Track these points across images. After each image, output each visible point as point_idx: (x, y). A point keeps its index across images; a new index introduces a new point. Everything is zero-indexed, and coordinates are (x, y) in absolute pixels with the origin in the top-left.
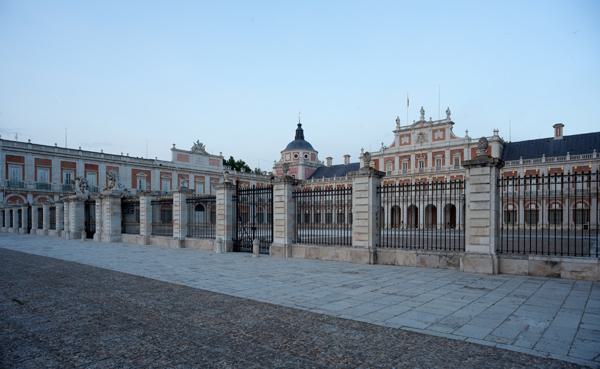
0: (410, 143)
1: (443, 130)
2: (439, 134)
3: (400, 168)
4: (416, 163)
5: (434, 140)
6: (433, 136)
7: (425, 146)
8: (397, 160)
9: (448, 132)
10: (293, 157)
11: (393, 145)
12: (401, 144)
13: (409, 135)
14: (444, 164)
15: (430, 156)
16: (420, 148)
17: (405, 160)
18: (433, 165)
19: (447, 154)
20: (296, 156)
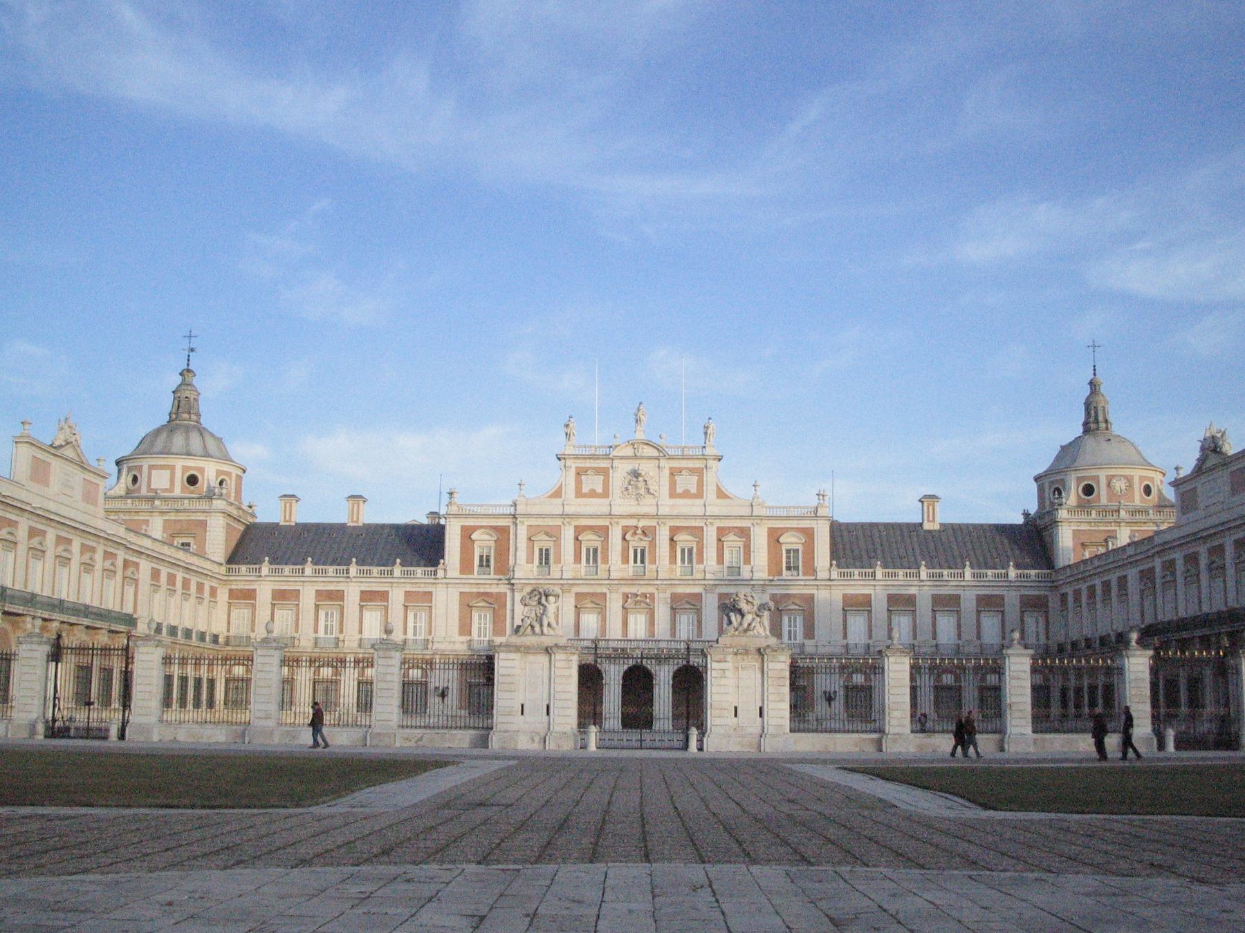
0: (606, 494)
1: (699, 472)
2: (687, 482)
3: (578, 559)
4: (625, 550)
5: (673, 494)
6: (673, 485)
7: (647, 507)
8: (568, 535)
9: (710, 479)
10: (180, 478)
11: (558, 494)
12: (579, 493)
13: (605, 472)
14: (700, 561)
15: (663, 535)
16: (634, 509)
17: (590, 540)
18: (673, 559)
19: (710, 535)
20: (192, 480)
